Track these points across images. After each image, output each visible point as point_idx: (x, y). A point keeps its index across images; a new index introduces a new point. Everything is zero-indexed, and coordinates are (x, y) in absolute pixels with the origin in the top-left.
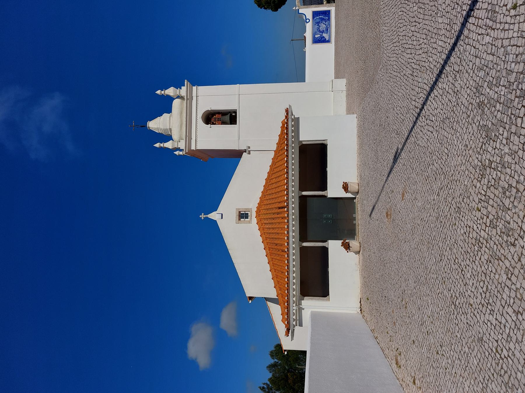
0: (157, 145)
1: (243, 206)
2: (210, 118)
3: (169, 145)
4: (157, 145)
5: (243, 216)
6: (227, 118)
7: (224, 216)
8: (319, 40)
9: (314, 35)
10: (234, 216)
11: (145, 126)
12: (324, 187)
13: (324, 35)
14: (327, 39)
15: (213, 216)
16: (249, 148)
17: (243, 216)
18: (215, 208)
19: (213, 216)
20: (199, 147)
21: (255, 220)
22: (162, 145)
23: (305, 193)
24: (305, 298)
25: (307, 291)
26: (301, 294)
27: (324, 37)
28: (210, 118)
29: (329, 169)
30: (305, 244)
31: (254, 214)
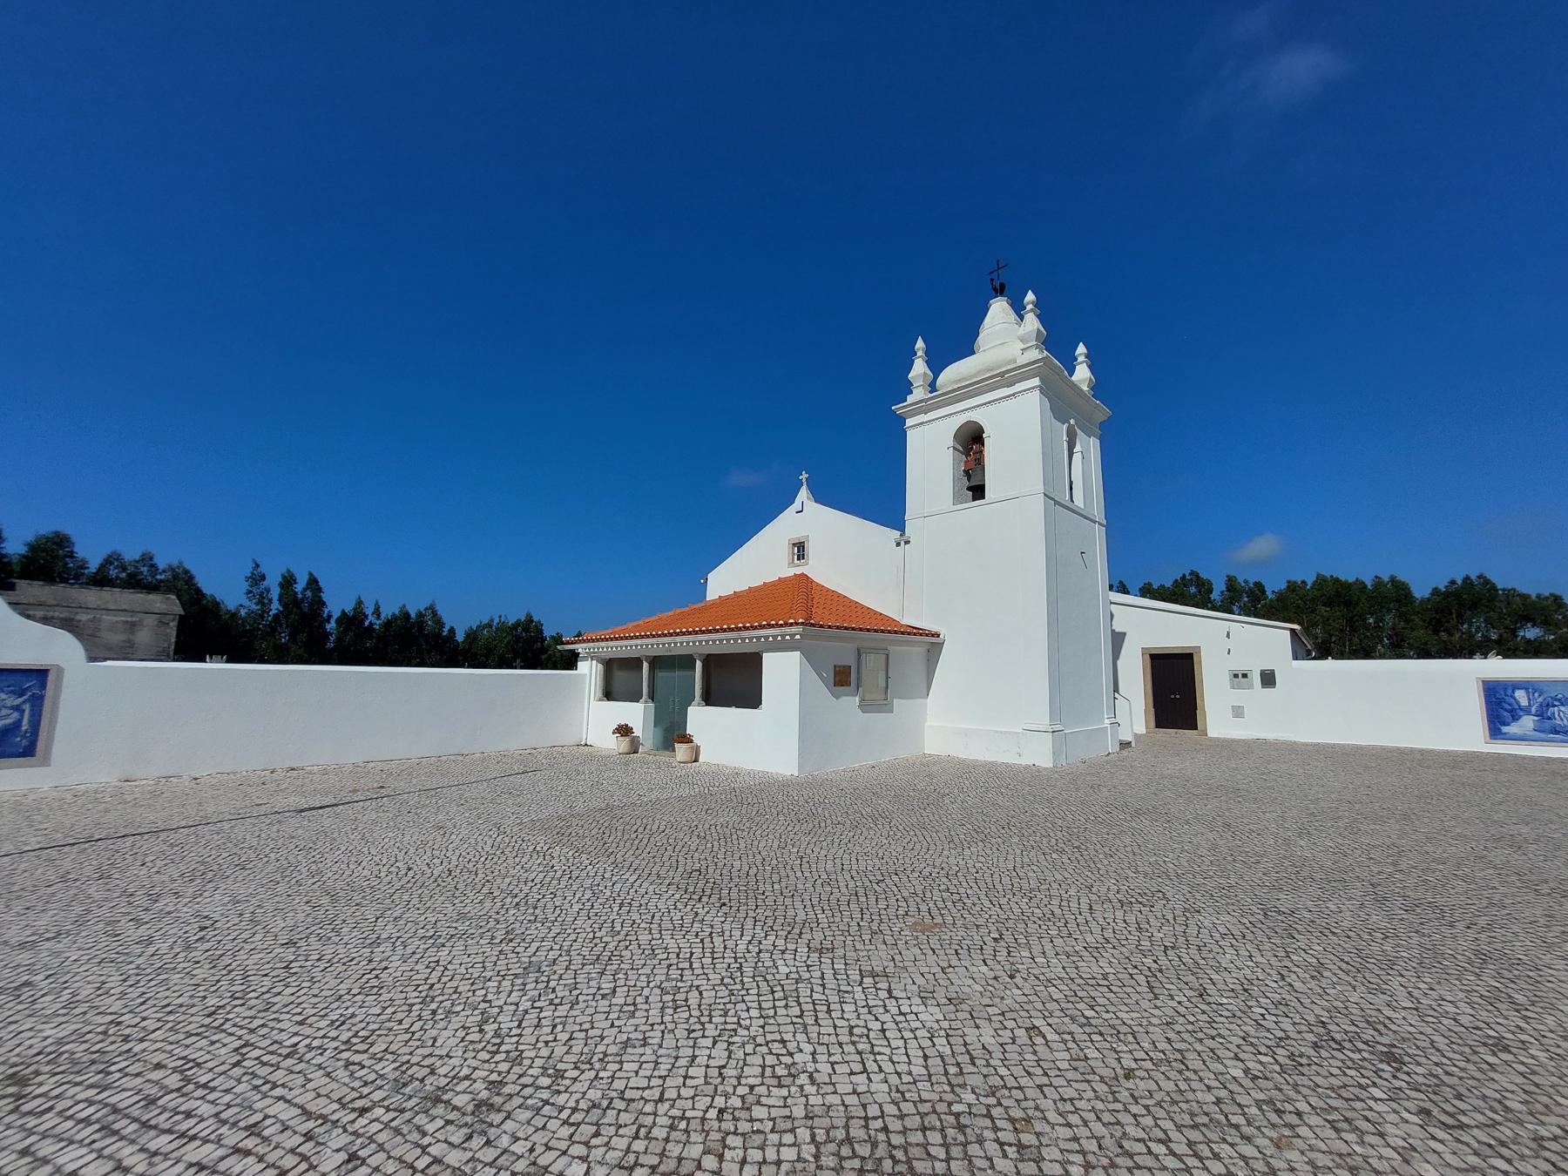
0: (920, 344)
1: (811, 550)
2: (972, 440)
3: (919, 368)
4: (920, 344)
5: (800, 549)
6: (975, 482)
7: (807, 517)
8: (1499, 705)
9: (1528, 686)
10: (797, 535)
11: (1000, 291)
12: (709, 699)
13: (1527, 723)
14: (1505, 729)
15: (804, 493)
16: (907, 542)
17: (800, 549)
18: (820, 497)
19: (804, 493)
20: (912, 437)
21: (791, 572)
22: (920, 353)
23: (699, 664)
24: (600, 667)
25: (611, 666)
26: (709, 655)
27: (1515, 718)
28: (972, 440)
29: (733, 710)
30: (645, 665)
31: (798, 571)
